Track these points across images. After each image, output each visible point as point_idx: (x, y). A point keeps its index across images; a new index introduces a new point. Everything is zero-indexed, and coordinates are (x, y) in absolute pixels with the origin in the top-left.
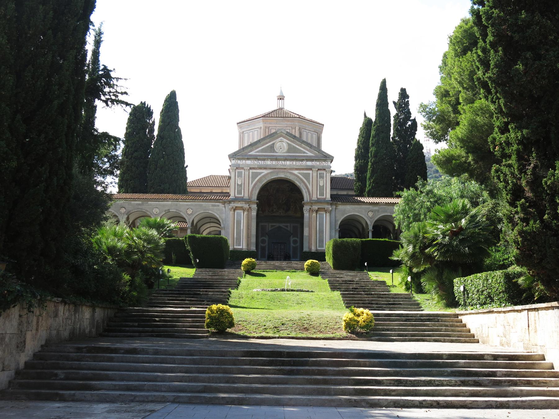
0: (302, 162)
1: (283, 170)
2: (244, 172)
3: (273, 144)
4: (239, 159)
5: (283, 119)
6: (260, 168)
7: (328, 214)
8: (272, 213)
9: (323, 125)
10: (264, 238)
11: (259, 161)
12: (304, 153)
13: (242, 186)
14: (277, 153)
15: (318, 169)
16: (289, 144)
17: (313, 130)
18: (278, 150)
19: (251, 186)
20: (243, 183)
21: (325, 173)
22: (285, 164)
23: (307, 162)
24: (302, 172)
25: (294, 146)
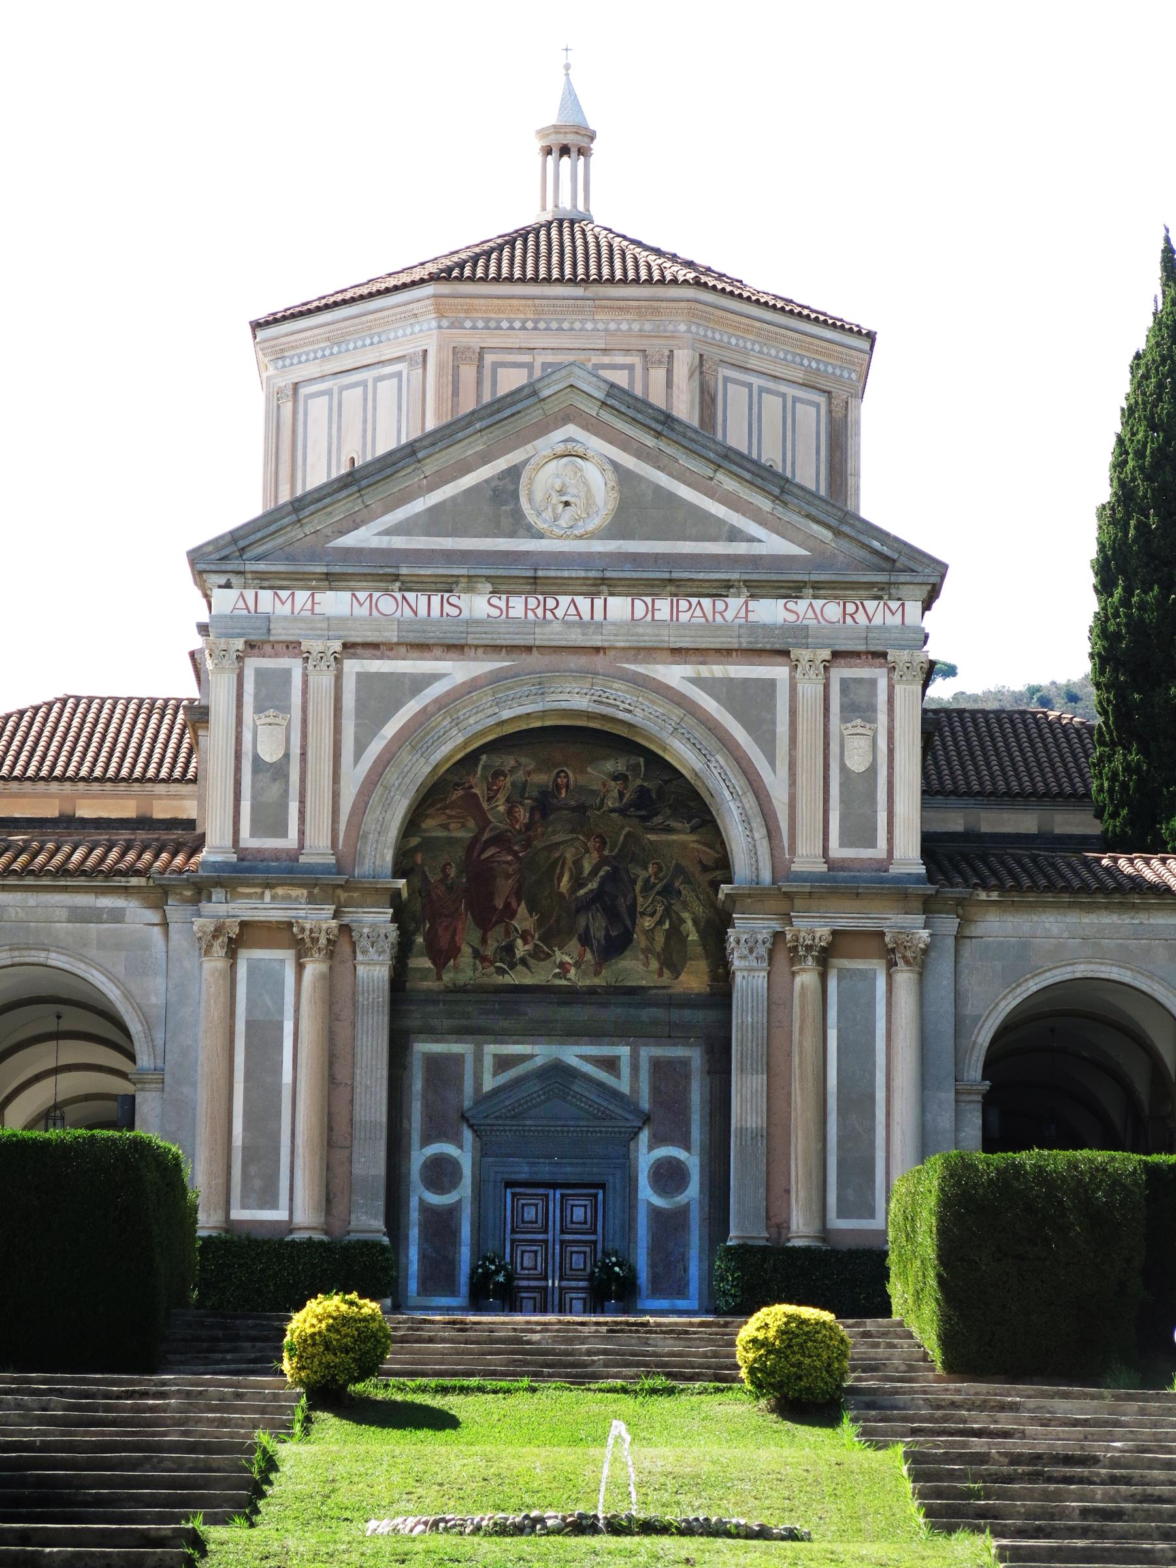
0: (720, 605)
1: (583, 661)
2: (305, 676)
3: (514, 473)
4: (264, 580)
5: (578, 291)
6: (421, 648)
7: (905, 978)
9: (871, 337)
10: (450, 1149)
11: (411, 596)
12: (735, 535)
13: (286, 777)
14: (541, 536)
15: (836, 654)
16: (623, 476)
17: (799, 376)
18: (548, 515)
19: (353, 777)
20: (296, 751)
21: (882, 684)
22: (599, 616)
23: (752, 604)
24: (718, 670)
25: (658, 489)
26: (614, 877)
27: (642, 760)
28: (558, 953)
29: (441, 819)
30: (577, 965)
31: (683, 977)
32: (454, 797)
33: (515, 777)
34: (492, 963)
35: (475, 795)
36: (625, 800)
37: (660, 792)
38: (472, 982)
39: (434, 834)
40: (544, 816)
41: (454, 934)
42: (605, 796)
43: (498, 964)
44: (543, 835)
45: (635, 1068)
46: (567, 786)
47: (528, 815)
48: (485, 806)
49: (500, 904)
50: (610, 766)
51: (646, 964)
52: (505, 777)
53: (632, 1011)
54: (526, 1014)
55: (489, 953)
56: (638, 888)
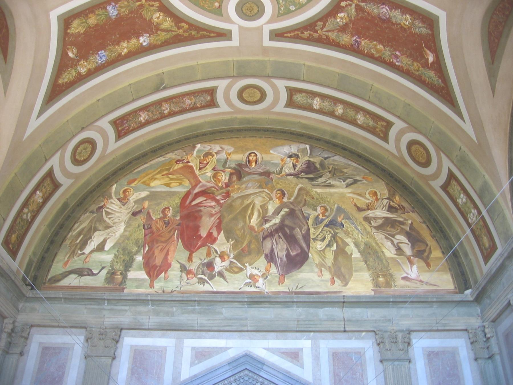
8: (202, 281)
26: (292, 213)
27: (308, 147)
28: (248, 268)
29: (166, 180)
30: (265, 276)
31: (351, 284)
32: (176, 168)
33: (219, 156)
34: (195, 275)
35: (191, 167)
36: (297, 169)
37: (322, 164)
38: (178, 289)
39: (159, 190)
40: (240, 178)
41: (167, 254)
42: (283, 166)
43: (200, 276)
44: (239, 189)
45: (316, 358)
46: (256, 161)
47: (228, 178)
48: (197, 172)
49: (204, 233)
50: (286, 149)
51: (321, 275)
52: (213, 156)
53: (312, 310)
54: (222, 313)
55: (193, 267)
56: (310, 222)
